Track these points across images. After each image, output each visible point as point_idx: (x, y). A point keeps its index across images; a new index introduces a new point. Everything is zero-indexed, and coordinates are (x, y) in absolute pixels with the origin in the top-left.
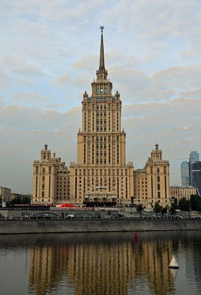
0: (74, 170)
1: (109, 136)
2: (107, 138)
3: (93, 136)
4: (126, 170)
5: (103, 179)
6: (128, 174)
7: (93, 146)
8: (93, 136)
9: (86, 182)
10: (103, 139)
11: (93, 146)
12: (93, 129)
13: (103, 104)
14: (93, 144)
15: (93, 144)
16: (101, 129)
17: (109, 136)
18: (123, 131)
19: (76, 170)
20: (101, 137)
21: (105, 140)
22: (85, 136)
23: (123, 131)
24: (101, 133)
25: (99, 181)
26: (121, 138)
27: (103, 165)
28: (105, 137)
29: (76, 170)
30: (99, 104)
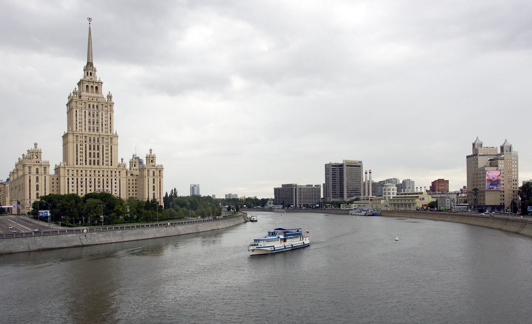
0: (66, 171)
1: (103, 138)
2: (101, 139)
3: (86, 137)
4: (120, 172)
5: (97, 180)
6: (121, 176)
7: (86, 147)
8: (86, 137)
9: (79, 183)
10: (96, 140)
11: (86, 147)
12: (85, 129)
13: (95, 104)
14: (86, 145)
15: (86, 145)
16: (94, 130)
17: (103, 138)
18: (116, 133)
19: (68, 170)
20: (94, 138)
21: (98, 141)
22: (77, 136)
23: (116, 133)
24: (94, 133)
25: (93, 182)
26: (114, 140)
27: (96, 166)
28: (98, 138)
29: (68, 170)
30: (92, 104)
